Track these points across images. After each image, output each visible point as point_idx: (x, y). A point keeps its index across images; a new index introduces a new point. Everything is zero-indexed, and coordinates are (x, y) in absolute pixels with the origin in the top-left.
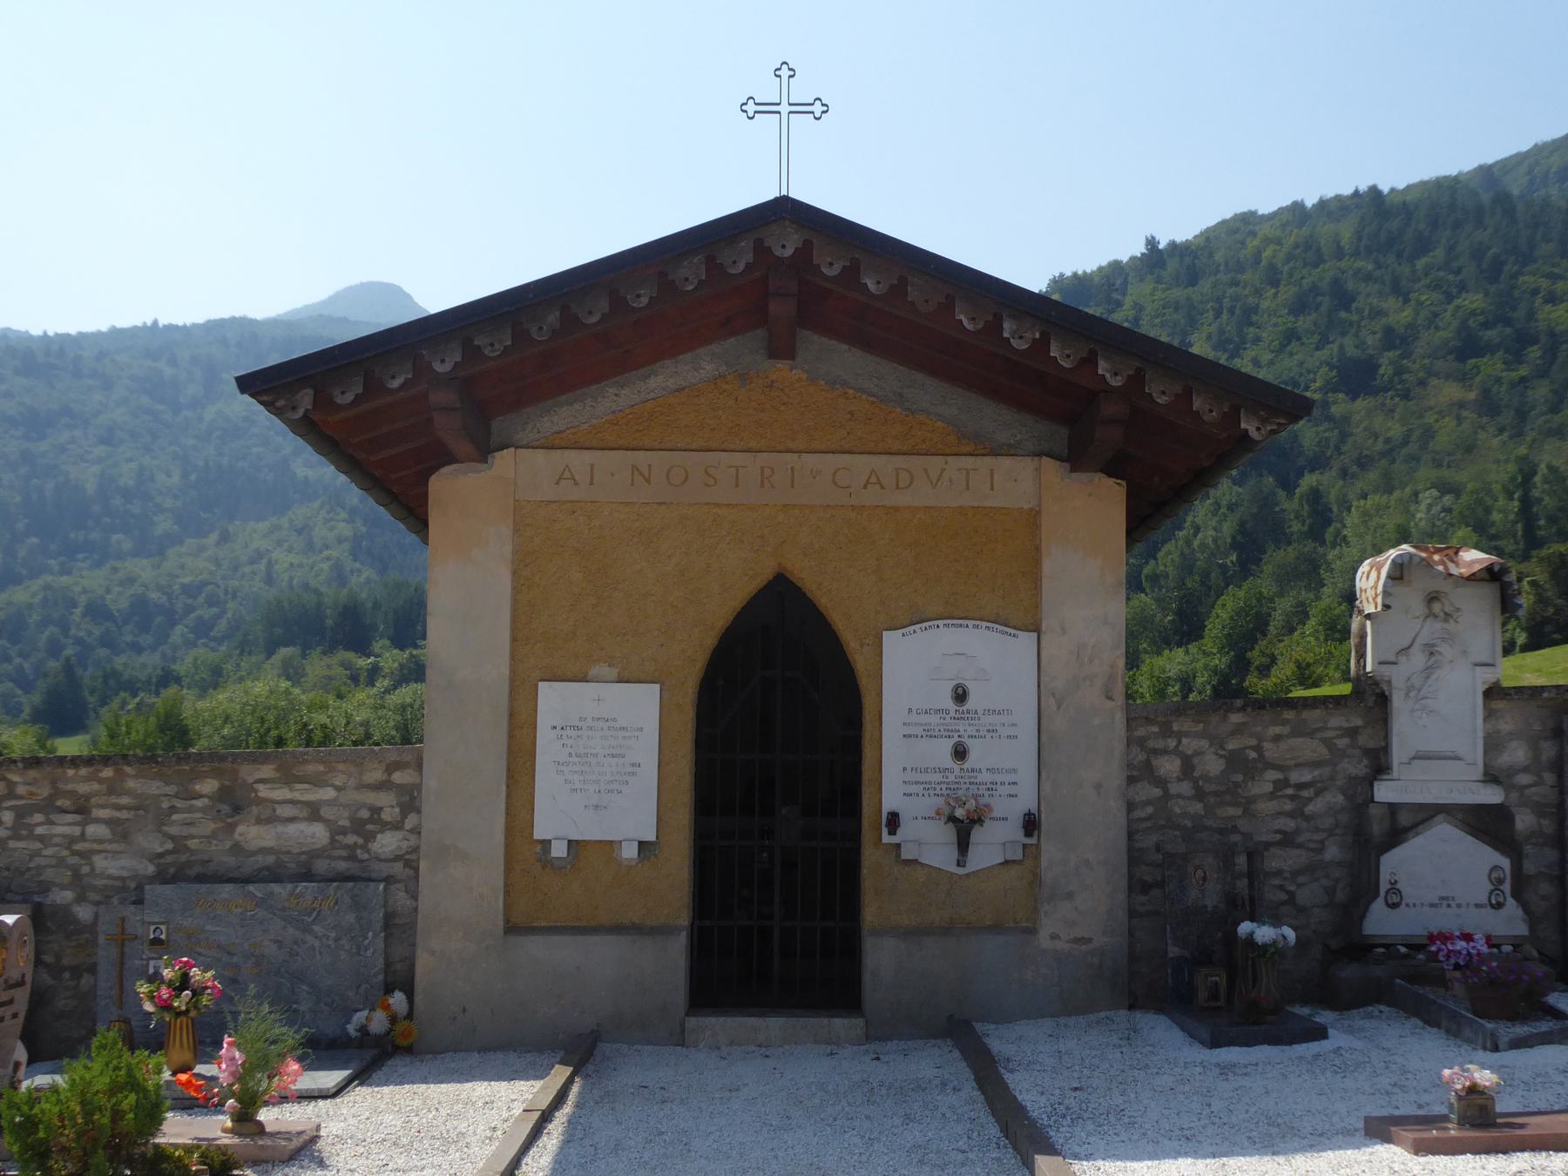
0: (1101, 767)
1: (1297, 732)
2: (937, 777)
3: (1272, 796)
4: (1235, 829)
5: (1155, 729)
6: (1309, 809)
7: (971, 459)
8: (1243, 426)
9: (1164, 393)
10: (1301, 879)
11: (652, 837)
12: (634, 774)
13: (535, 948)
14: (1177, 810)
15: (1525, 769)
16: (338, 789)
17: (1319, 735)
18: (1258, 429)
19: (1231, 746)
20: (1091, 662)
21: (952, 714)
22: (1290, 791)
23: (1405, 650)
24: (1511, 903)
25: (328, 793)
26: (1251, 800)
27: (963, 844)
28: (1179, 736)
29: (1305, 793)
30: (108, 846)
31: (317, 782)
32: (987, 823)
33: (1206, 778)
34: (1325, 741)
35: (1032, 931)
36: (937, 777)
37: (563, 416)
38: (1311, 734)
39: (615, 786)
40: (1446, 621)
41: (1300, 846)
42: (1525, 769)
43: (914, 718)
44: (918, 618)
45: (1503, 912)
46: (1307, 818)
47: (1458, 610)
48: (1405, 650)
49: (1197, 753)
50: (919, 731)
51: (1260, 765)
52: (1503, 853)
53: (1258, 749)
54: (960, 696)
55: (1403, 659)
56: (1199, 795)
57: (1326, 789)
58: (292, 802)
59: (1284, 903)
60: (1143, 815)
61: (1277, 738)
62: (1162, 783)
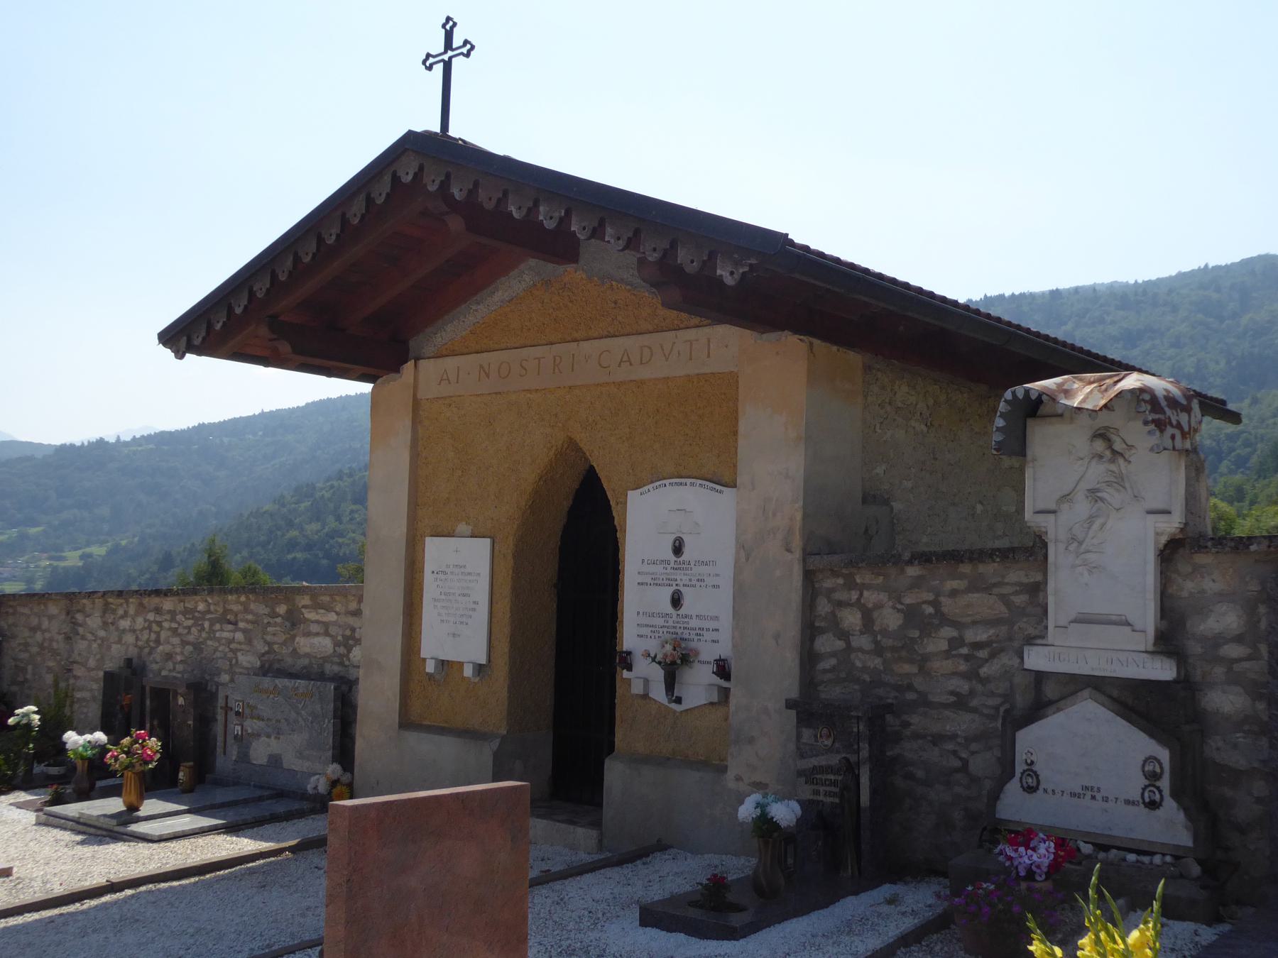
0: (783, 620)
1: (973, 588)
2: (660, 622)
3: (947, 654)
4: (910, 687)
5: (841, 581)
6: (984, 671)
7: (694, 331)
8: (719, 272)
9: (655, 250)
10: (974, 747)
11: (484, 662)
12: (474, 610)
13: (412, 737)
14: (859, 664)
15: (1239, 639)
16: (338, 614)
17: (995, 590)
18: (732, 273)
19: (908, 600)
20: (774, 515)
21: (672, 565)
22: (964, 651)
23: (1066, 498)
24: (1170, 804)
25: (332, 617)
26: (926, 658)
27: (671, 682)
28: (862, 588)
29: (982, 654)
30: (243, 647)
31: (328, 609)
32: (696, 665)
33: (885, 632)
34: (1004, 599)
35: (723, 769)
36: (660, 622)
37: (453, 329)
38: (987, 589)
39: (464, 619)
40: (1112, 461)
41: (974, 710)
42: (1239, 639)
43: (646, 568)
44: (657, 476)
45: (1160, 813)
46: (984, 681)
47: (1131, 447)
48: (1066, 498)
49: (879, 606)
50: (649, 581)
51: (936, 622)
52: (1161, 741)
53: (935, 604)
54: (678, 549)
55: (1065, 507)
56: (879, 650)
57: (1002, 650)
58: (318, 622)
59: (957, 770)
60: (827, 666)
61: (954, 593)
62: (844, 635)
